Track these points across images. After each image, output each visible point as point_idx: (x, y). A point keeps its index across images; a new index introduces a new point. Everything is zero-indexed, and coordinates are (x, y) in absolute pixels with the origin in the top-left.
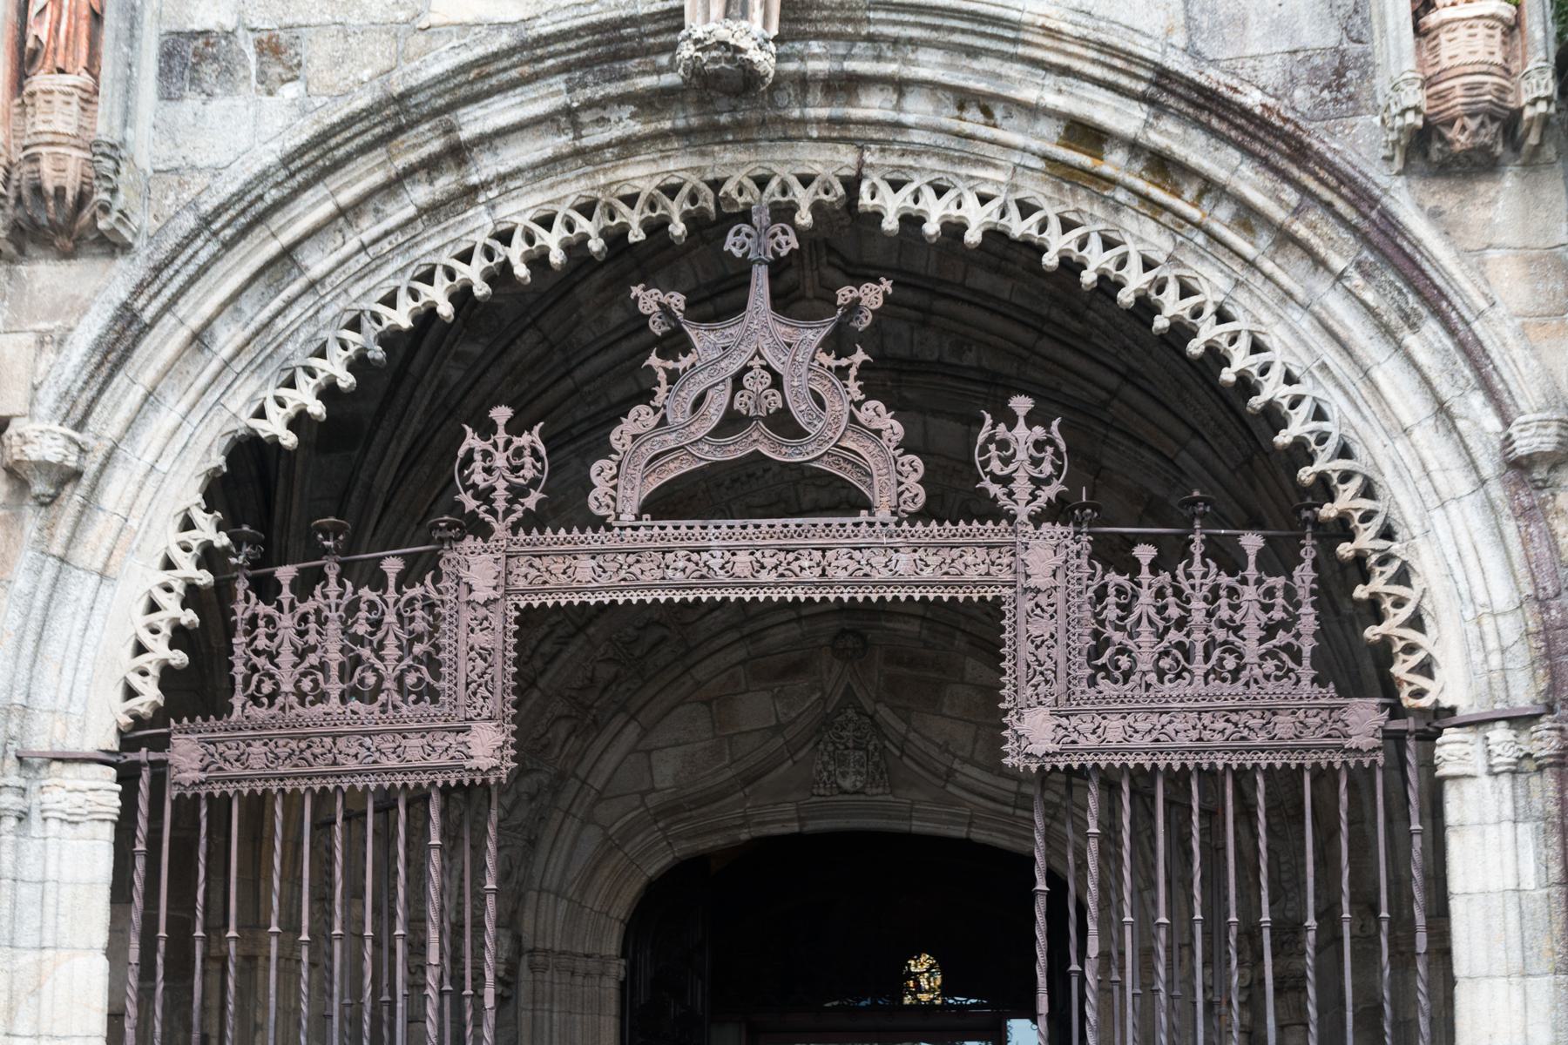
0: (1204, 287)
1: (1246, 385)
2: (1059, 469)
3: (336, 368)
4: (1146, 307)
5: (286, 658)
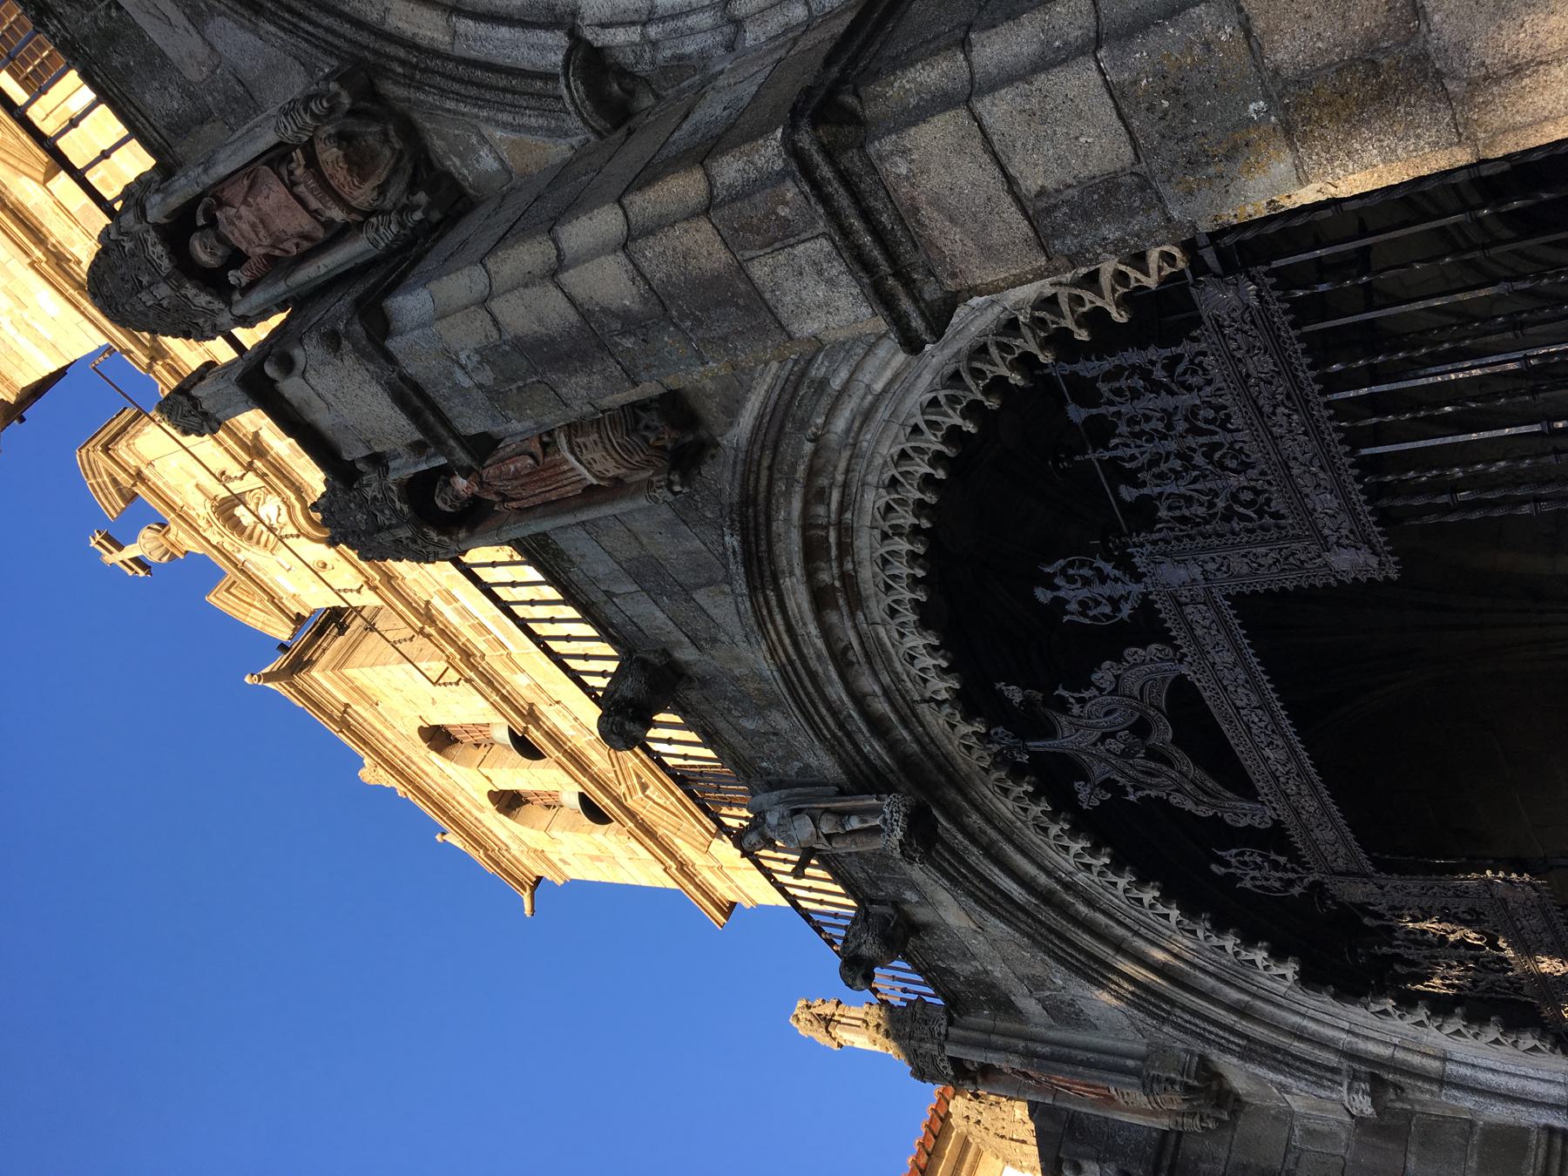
0: (881, 503)
2: (1082, 564)
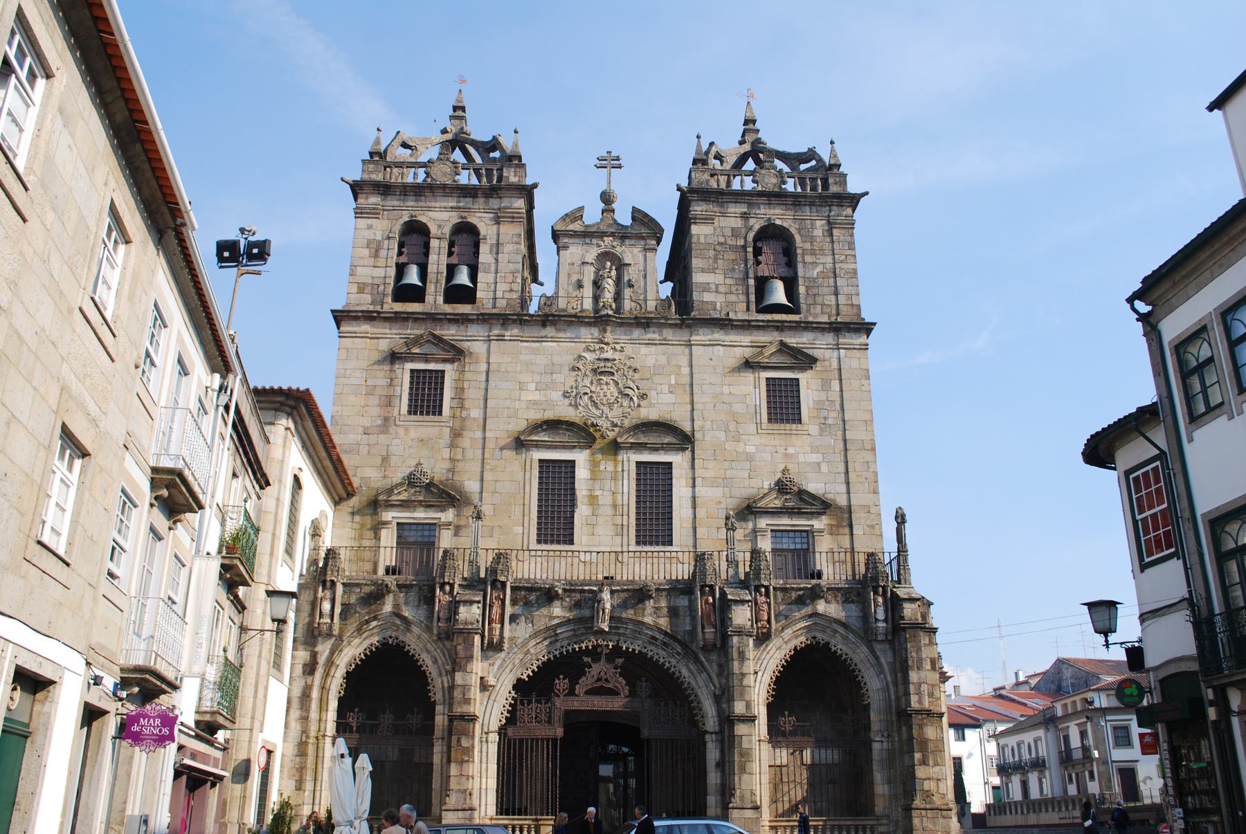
1: (678, 678)
3: (535, 668)
4: (663, 664)
5: (526, 716)
